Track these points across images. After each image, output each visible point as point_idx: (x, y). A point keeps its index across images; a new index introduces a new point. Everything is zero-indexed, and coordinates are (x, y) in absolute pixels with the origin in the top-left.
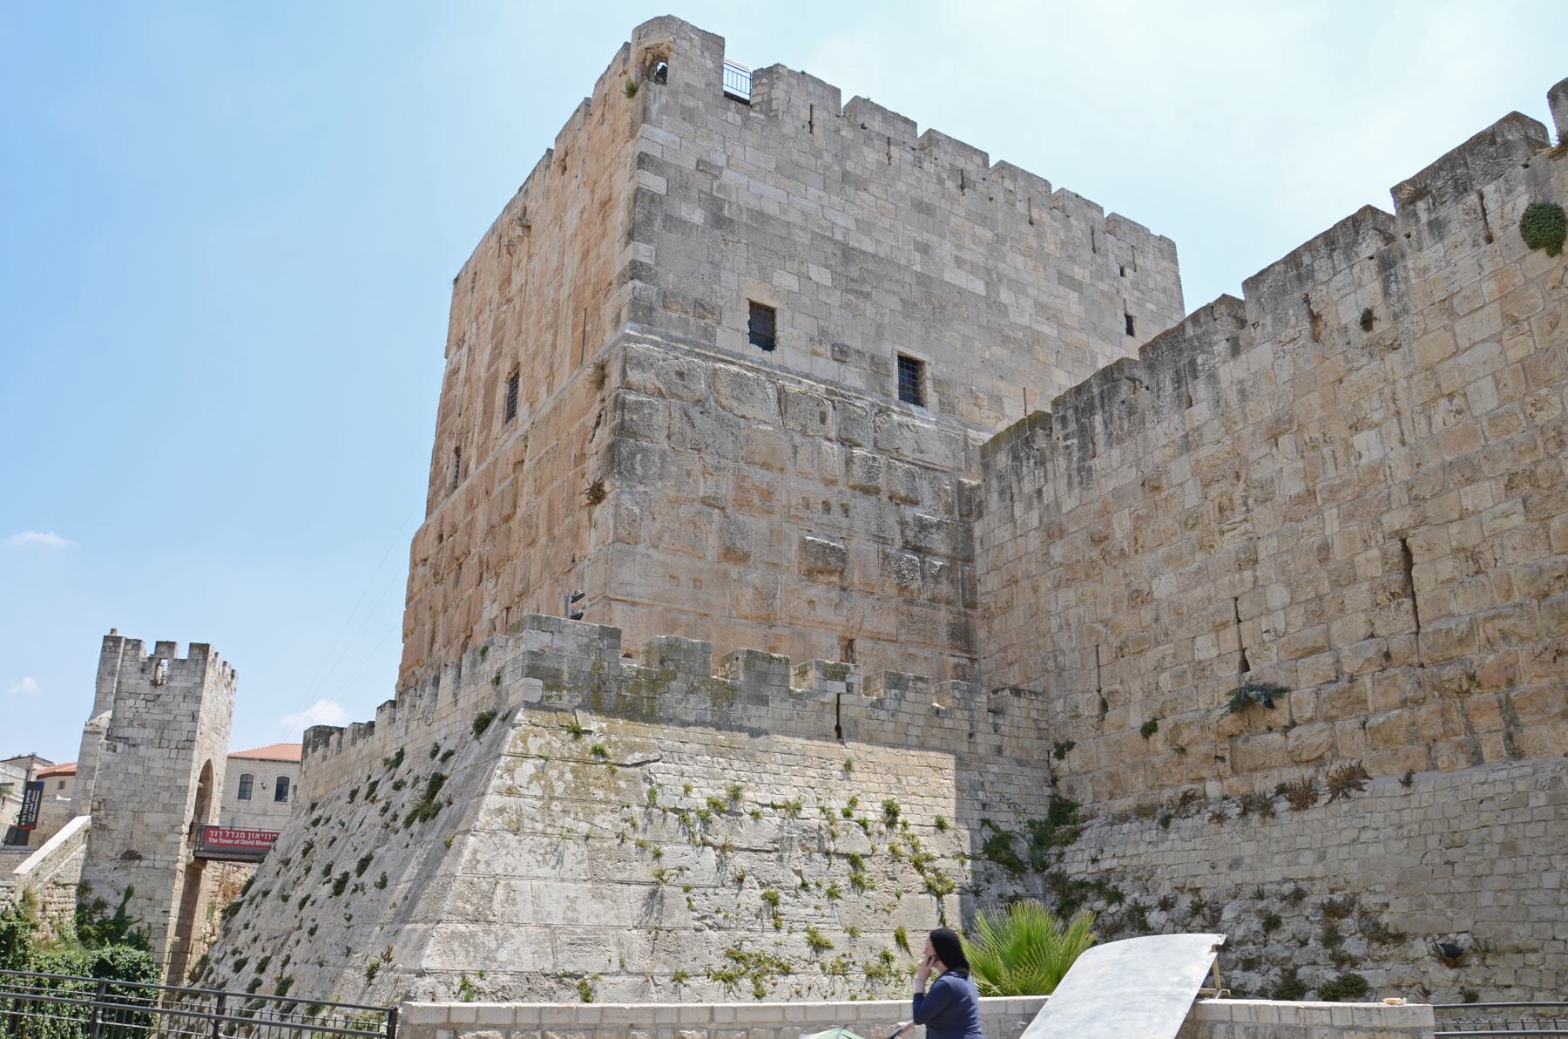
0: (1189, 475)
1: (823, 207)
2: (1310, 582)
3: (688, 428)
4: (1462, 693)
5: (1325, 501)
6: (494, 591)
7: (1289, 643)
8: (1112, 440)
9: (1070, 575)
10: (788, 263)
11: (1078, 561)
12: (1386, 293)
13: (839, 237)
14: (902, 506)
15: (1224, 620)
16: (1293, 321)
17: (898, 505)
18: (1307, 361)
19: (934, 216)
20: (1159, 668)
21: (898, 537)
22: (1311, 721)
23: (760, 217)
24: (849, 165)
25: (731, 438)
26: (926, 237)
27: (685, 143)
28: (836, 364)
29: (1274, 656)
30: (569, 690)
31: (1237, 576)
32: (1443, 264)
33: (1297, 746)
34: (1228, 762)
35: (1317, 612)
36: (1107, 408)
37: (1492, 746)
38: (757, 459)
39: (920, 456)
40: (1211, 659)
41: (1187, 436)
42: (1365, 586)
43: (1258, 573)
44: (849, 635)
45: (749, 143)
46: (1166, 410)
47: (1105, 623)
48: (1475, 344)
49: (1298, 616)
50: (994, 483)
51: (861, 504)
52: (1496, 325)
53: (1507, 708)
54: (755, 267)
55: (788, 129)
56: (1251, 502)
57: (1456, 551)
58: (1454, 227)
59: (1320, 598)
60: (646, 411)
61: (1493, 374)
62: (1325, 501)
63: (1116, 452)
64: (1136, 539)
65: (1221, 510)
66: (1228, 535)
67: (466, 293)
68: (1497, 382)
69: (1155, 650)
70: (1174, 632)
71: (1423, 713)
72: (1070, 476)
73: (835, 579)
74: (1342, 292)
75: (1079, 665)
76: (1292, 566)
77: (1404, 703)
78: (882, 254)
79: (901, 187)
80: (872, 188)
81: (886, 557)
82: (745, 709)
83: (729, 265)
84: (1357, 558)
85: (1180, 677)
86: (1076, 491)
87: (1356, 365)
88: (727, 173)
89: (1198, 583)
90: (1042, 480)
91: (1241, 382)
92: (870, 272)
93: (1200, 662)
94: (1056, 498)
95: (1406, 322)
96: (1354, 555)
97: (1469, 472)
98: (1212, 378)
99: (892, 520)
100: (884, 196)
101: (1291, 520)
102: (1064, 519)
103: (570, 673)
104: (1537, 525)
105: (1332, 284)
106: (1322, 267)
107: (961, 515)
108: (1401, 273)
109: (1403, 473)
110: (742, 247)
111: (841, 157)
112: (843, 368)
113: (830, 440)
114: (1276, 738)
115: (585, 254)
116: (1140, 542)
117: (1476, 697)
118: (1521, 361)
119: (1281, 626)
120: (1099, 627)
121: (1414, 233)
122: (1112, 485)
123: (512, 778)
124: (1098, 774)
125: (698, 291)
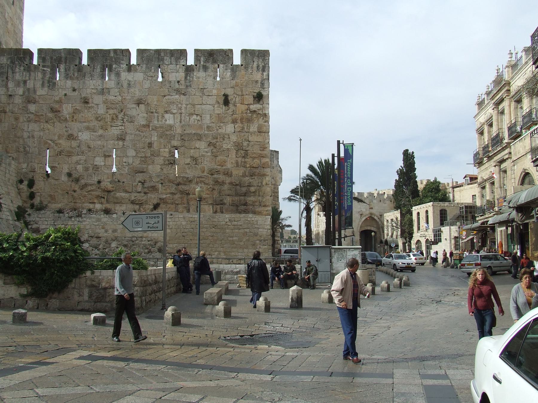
2: (143, 152)
5: (153, 129)
9: (38, 118)
11: (43, 115)
12: (186, 78)
15: (109, 155)
16: (153, 71)
20: (78, 163)
32: (204, 79)
33: (135, 199)
35: (144, 160)
40: (101, 165)
41: (103, 89)
42: (162, 158)
43: (125, 144)
46: (96, 77)
47: (53, 141)
48: (207, 104)
49: (137, 161)
52: (214, 102)
56: (125, 120)
57: (191, 157)
58: (210, 70)
59: (146, 157)
62: (153, 129)
64: (73, 117)
65: (113, 119)
66: (113, 128)
68: (211, 117)
70: (86, 153)
71: (176, 197)
72: (43, 82)
74: (172, 71)
75: (37, 153)
76: (138, 145)
84: (161, 150)
85: (87, 169)
86: (46, 89)
89: (100, 140)
90: (27, 78)
91: (130, 81)
93: (96, 165)
94: (34, 88)
95: (189, 89)
97: (199, 137)
98: (118, 75)
102: (37, 97)
105: (169, 66)
106: (167, 60)
108: (192, 75)
116: (75, 118)
118: (218, 114)
120: (50, 142)
121: (198, 66)
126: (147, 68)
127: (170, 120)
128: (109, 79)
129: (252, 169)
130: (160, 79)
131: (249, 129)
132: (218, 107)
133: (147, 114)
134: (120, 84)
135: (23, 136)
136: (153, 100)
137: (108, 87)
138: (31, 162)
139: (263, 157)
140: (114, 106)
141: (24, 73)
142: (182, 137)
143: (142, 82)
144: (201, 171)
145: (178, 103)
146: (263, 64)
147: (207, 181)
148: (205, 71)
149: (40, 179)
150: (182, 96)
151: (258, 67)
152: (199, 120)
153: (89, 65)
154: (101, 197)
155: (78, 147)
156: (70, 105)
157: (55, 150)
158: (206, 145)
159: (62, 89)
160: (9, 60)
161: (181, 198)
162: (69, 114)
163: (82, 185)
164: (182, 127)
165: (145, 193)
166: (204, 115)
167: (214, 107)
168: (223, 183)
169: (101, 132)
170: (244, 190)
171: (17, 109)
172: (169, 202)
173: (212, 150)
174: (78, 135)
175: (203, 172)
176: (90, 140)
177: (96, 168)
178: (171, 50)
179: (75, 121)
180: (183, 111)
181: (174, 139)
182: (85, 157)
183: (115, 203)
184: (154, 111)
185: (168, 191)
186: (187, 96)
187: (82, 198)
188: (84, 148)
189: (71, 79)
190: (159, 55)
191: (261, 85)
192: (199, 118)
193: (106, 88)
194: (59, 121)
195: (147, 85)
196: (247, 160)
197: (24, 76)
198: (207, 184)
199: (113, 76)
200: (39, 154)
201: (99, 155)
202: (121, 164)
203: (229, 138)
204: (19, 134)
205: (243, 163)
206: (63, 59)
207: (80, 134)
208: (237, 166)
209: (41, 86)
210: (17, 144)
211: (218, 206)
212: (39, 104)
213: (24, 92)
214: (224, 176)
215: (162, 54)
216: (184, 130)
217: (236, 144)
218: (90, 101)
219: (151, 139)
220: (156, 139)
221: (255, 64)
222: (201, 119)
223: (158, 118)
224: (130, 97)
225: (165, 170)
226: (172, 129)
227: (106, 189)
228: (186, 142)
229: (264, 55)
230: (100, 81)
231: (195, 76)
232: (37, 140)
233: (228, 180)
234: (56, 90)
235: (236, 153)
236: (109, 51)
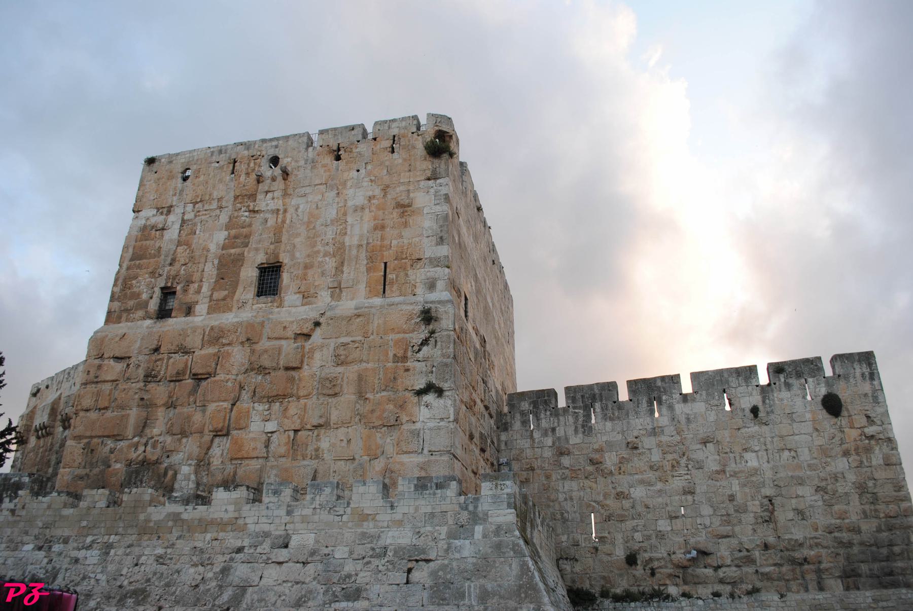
0: (654, 446)
2: (723, 508)
4: (801, 564)
5: (731, 476)
7: (713, 530)
8: (605, 418)
9: (574, 473)
11: (580, 469)
12: (764, 402)
15: (677, 515)
18: (724, 416)
20: (635, 530)
22: (729, 566)
29: (704, 536)
31: (683, 497)
32: (790, 400)
34: (681, 578)
35: (727, 520)
36: (604, 402)
37: (812, 586)
40: (667, 531)
41: (654, 429)
42: (752, 515)
43: (695, 498)
46: (642, 414)
47: (598, 503)
48: (801, 434)
49: (717, 521)
50: (518, 416)
52: (810, 430)
53: (819, 572)
56: (690, 466)
57: (794, 510)
59: (728, 515)
61: (809, 447)
62: (731, 476)
63: (609, 424)
64: (620, 468)
65: (673, 466)
66: (675, 478)
68: (810, 451)
69: (631, 522)
71: (784, 569)
72: (576, 427)
74: (742, 395)
75: (579, 520)
76: (714, 499)
77: (775, 565)
86: (581, 435)
87: (747, 425)
89: (660, 496)
90: (556, 424)
91: (688, 415)
93: (660, 531)
95: (772, 416)
96: (747, 501)
97: (801, 482)
98: (671, 408)
101: (712, 479)
102: (571, 447)
104: (827, 507)
105: (737, 389)
106: (733, 382)
108: (771, 397)
109: (769, 474)
114: (709, 571)
116: (623, 469)
117: (806, 567)
118: (820, 446)
119: (708, 523)
120: (594, 504)
121: (777, 384)
122: (604, 438)
124: (593, 575)
126: (707, 394)
127: (752, 461)
128: (660, 415)
129: (888, 519)
130: (728, 408)
131: (871, 462)
132: (818, 436)
133: (719, 455)
134: (676, 420)
135: (558, 499)
136: (725, 435)
137: (661, 425)
138: (572, 532)
139: (902, 500)
140: (672, 449)
141: (552, 419)
142: (776, 483)
143: (705, 414)
144: (813, 529)
145: (759, 437)
146: (869, 370)
147: (825, 543)
148: (789, 390)
149: (588, 555)
150: (764, 427)
151: (863, 375)
152: (794, 457)
153: (631, 400)
154: (675, 576)
155: (632, 508)
156: (614, 453)
157: (603, 514)
158: (813, 491)
159: (601, 433)
160: (532, 405)
161: (793, 570)
162: (614, 465)
163: (646, 561)
164: (772, 469)
165: (738, 566)
166: (800, 450)
167: (812, 436)
168: (850, 544)
169: (659, 486)
170: (884, 551)
171: (547, 465)
172: (775, 578)
173: (822, 497)
174: (629, 492)
175: (816, 530)
176: (647, 497)
177: (661, 536)
178: (737, 369)
179: (622, 473)
180: (769, 446)
181: (764, 486)
182: (643, 521)
183: (695, 583)
184: (728, 450)
185: (771, 562)
186: (771, 426)
187: (648, 579)
188: (640, 509)
189: (610, 420)
190: (722, 376)
191: (873, 400)
192: (793, 453)
193: (658, 427)
194: (603, 476)
195: (712, 417)
196: (878, 507)
197: (552, 422)
198: (826, 547)
199: (664, 410)
200: (582, 521)
201: (662, 517)
202: (695, 527)
203: (844, 477)
204: (552, 497)
205: (873, 512)
206: (597, 396)
207: (632, 490)
208: (866, 517)
209: (573, 433)
210: (551, 510)
211: (849, 580)
212: (574, 455)
213: (554, 443)
214: (850, 534)
215: (726, 375)
216: (776, 473)
217: (857, 486)
218: (640, 446)
219: (731, 489)
220: (738, 489)
221: (858, 372)
222: (797, 455)
223: (736, 460)
224: (691, 436)
225: (759, 531)
226: (759, 473)
227: (680, 564)
228: (782, 489)
229: (867, 358)
230: (648, 418)
231: (776, 399)
232: (577, 503)
233: (856, 538)
234: (594, 435)
235: (859, 498)
236: (655, 379)
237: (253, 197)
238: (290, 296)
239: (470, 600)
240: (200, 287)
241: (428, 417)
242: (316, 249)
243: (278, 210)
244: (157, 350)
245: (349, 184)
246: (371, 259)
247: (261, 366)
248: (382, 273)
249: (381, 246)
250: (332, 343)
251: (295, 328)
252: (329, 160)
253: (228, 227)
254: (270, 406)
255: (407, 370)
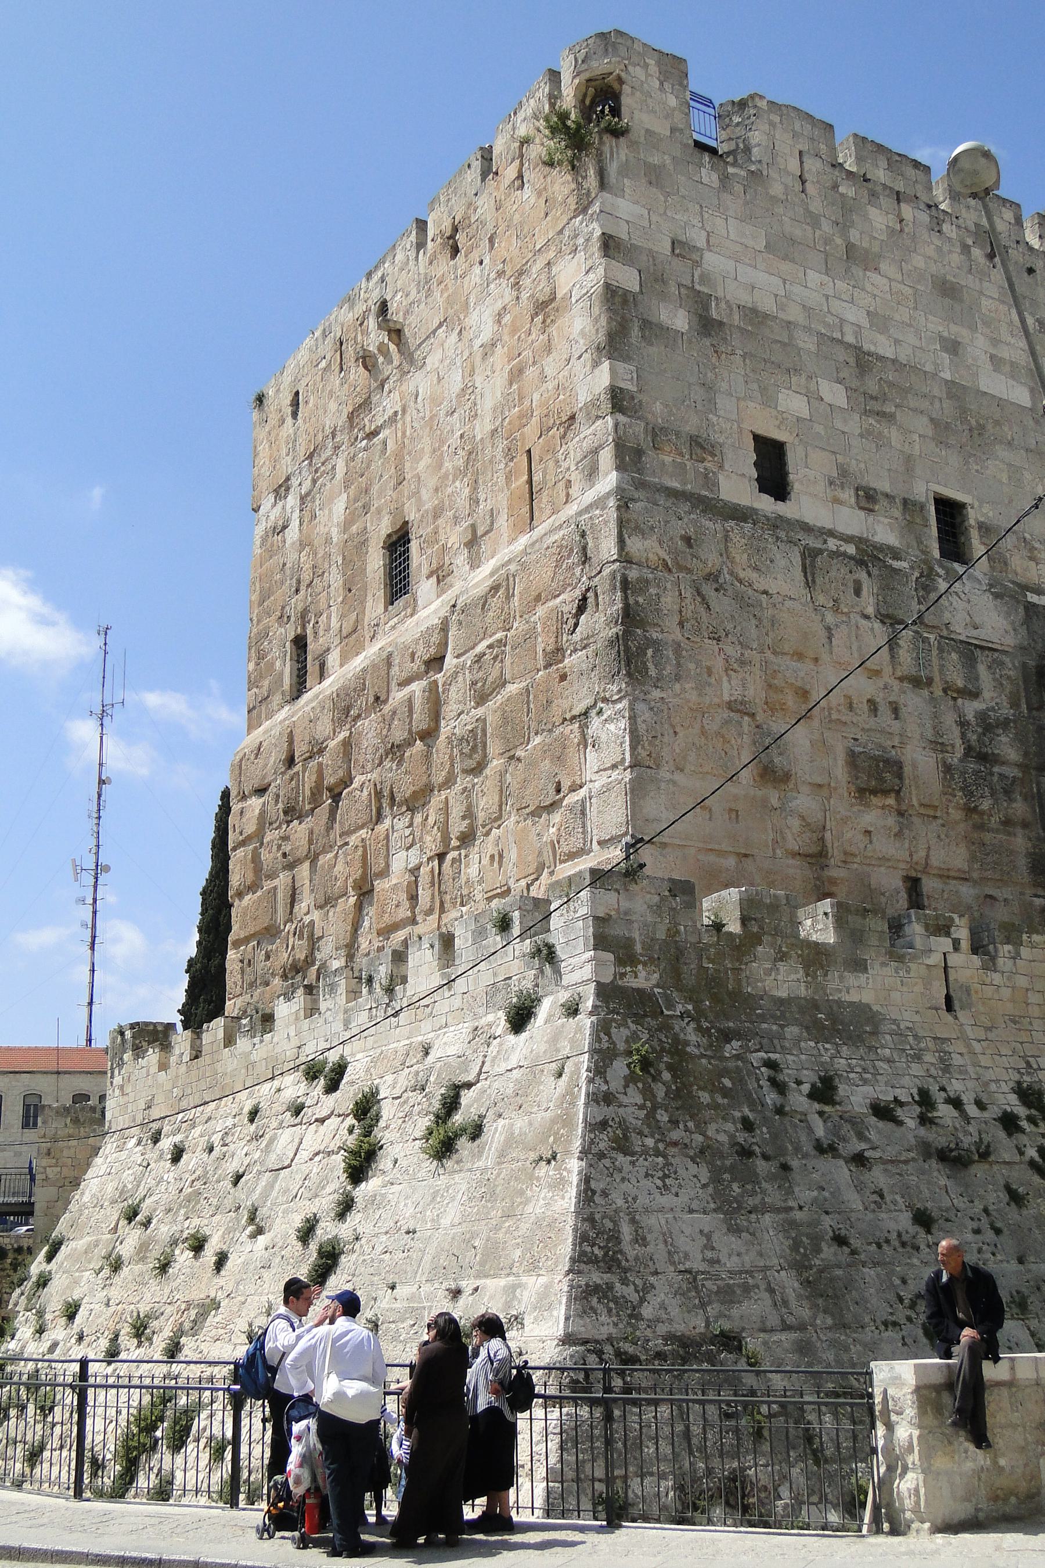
1: (827, 297)
3: (702, 610)
6: (407, 832)
10: (794, 379)
13: (850, 339)
14: (960, 701)
17: (955, 699)
19: (961, 301)
21: (958, 742)
23: (755, 316)
24: (854, 236)
25: (754, 622)
26: (956, 330)
27: (654, 218)
28: (862, 514)
30: (645, 964)
38: (786, 649)
39: (975, 633)
44: (914, 874)
45: (731, 213)
51: (914, 702)
54: (755, 386)
55: (777, 189)
60: (653, 591)
67: (283, 421)
73: (891, 801)
78: (903, 359)
79: (918, 261)
80: (883, 266)
81: (948, 769)
82: (841, 977)
83: (724, 386)
88: (708, 256)
92: (891, 385)
99: (949, 719)
100: (899, 277)
103: (643, 943)
107: (1030, 709)
110: (738, 359)
111: (843, 226)
112: (871, 519)
113: (867, 617)
115: (516, 374)
123: (606, 1082)
125: (691, 425)
237: (365, 405)
238: (424, 587)
239: (487, 1158)
240: (329, 618)
241: (596, 769)
242: (443, 470)
243: (396, 413)
244: (290, 761)
245: (472, 300)
246: (509, 454)
247: (393, 744)
248: (526, 477)
249: (521, 416)
250: (468, 659)
251: (424, 653)
252: (444, 265)
253: (347, 484)
254: (412, 818)
255: (563, 677)
